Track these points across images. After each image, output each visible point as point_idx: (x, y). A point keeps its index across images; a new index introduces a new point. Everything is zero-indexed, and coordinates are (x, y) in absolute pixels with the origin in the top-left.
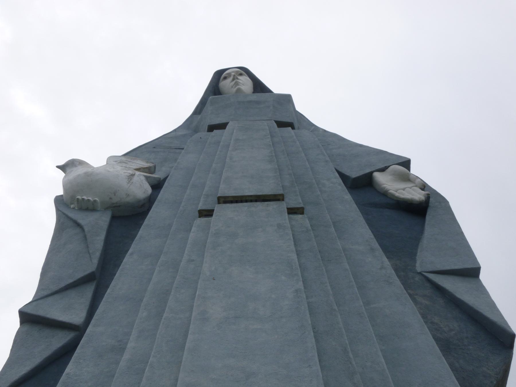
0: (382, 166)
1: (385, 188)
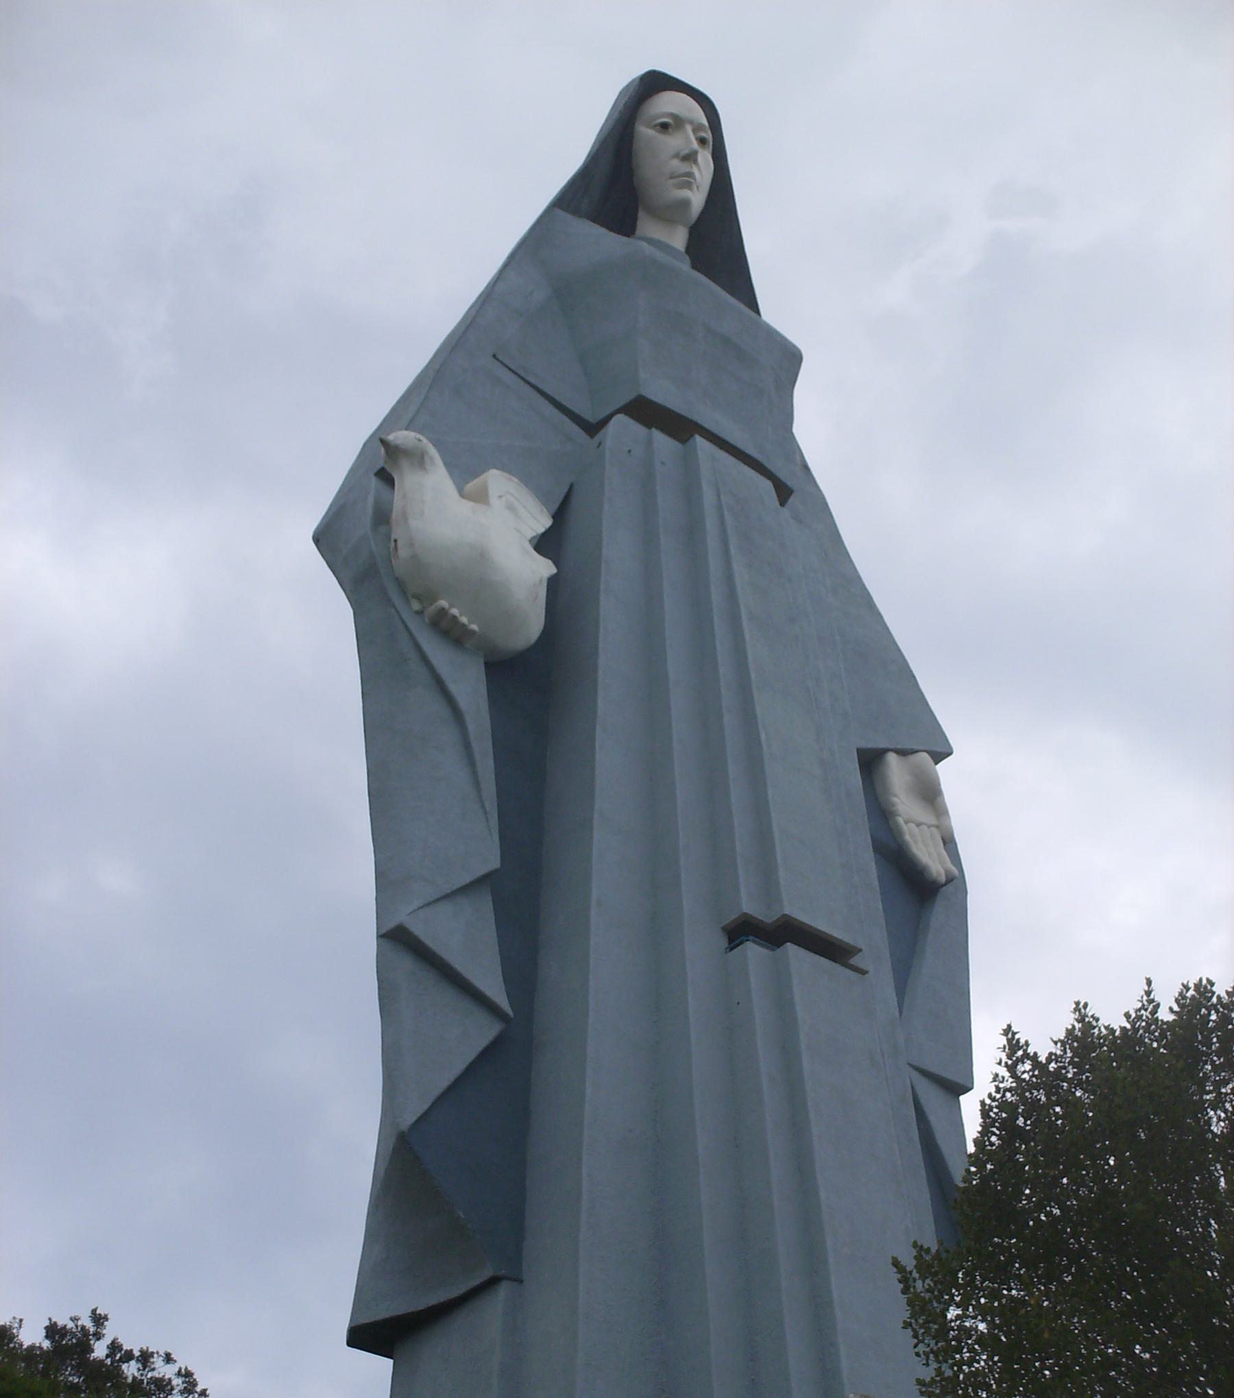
0: (907, 745)
1: (893, 805)
